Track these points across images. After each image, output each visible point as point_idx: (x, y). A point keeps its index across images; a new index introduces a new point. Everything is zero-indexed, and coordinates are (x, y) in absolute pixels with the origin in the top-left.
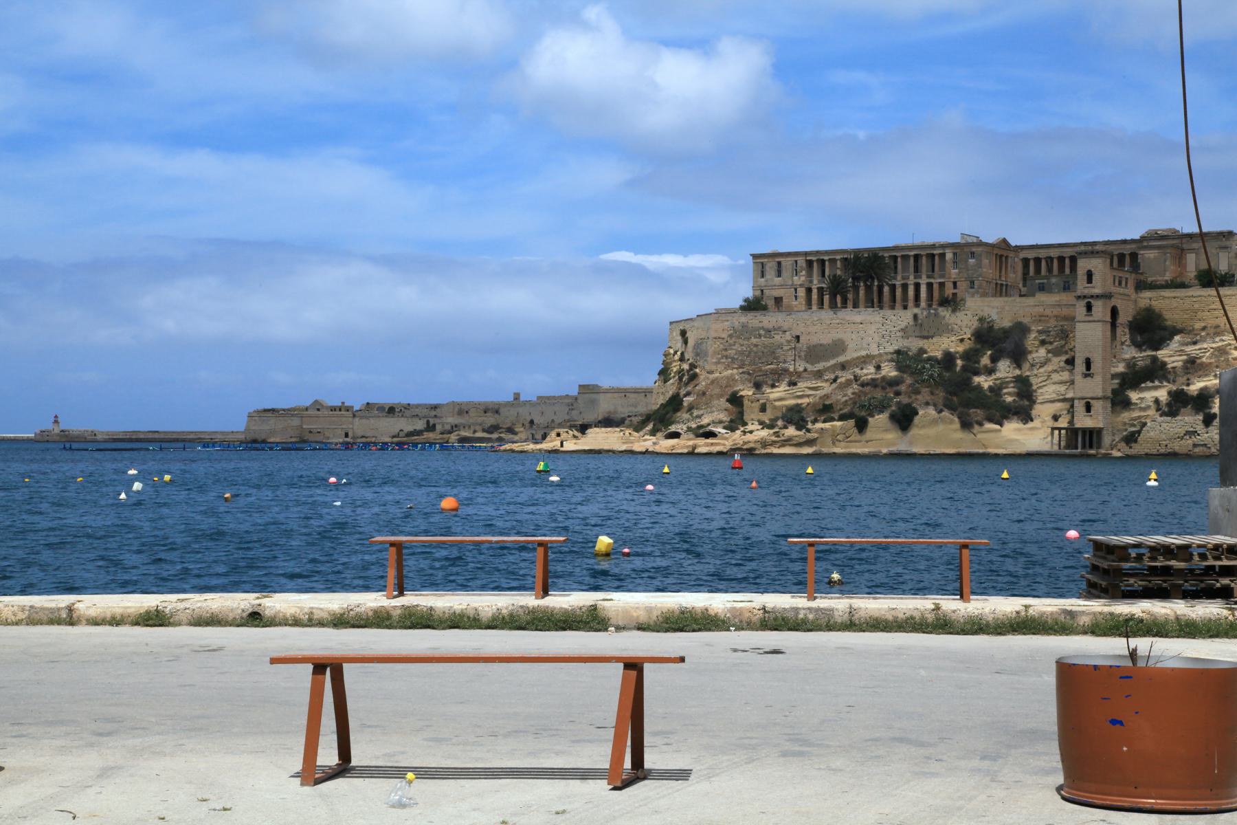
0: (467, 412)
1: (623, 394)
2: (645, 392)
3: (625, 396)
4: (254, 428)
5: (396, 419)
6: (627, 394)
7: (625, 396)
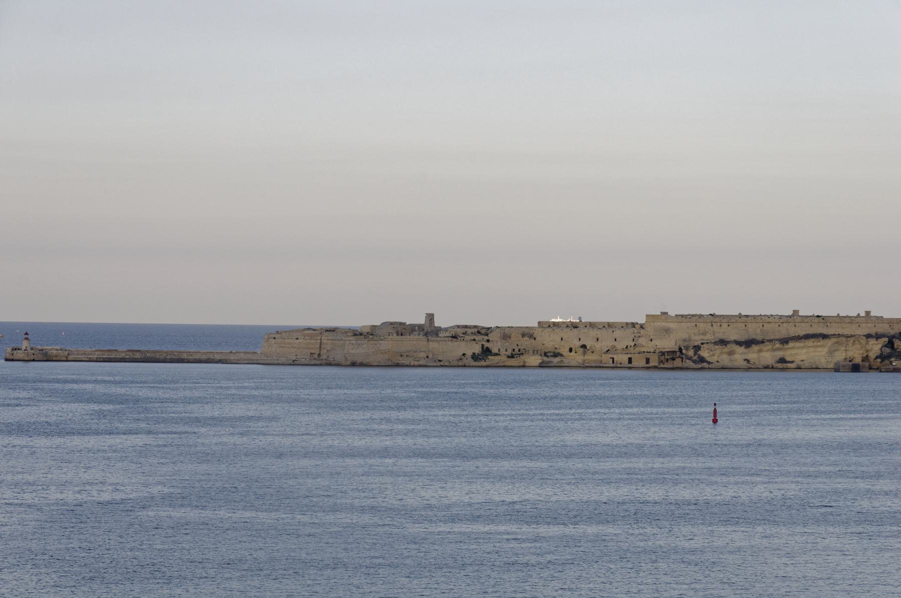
4: (352, 352)
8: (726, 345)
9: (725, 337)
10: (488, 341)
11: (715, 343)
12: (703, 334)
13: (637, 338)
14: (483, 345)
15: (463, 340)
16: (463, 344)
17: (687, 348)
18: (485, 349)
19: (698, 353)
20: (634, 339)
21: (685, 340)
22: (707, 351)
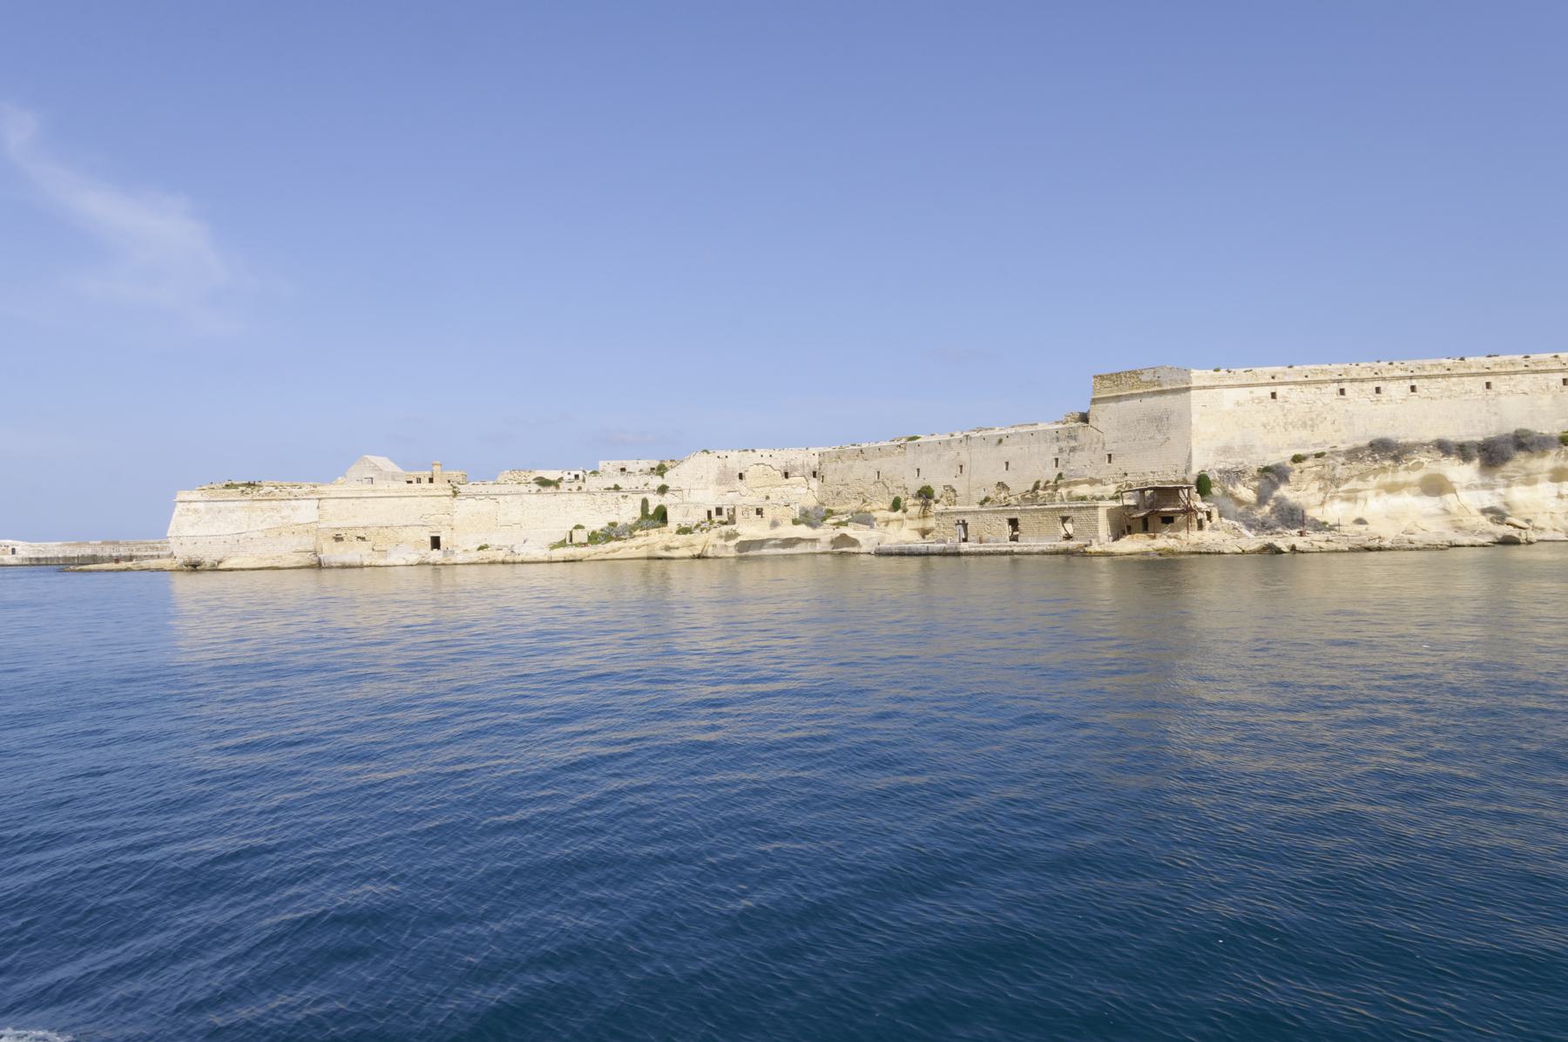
0: (741, 476)
1: (1268, 391)
2: (1339, 381)
3: (1274, 395)
5: (564, 497)
6: (1280, 390)
7: (1274, 395)
8: (1396, 459)
9: (1400, 433)
10: (663, 490)
11: (1353, 454)
12: (1304, 425)
13: (1065, 455)
14: (645, 502)
15: (580, 488)
16: (578, 499)
17: (1235, 475)
18: (651, 512)
19: (1276, 494)
20: (1057, 460)
21: (1226, 450)
22: (1317, 484)
